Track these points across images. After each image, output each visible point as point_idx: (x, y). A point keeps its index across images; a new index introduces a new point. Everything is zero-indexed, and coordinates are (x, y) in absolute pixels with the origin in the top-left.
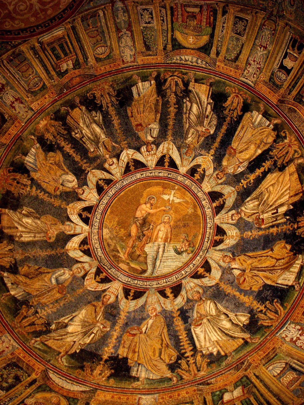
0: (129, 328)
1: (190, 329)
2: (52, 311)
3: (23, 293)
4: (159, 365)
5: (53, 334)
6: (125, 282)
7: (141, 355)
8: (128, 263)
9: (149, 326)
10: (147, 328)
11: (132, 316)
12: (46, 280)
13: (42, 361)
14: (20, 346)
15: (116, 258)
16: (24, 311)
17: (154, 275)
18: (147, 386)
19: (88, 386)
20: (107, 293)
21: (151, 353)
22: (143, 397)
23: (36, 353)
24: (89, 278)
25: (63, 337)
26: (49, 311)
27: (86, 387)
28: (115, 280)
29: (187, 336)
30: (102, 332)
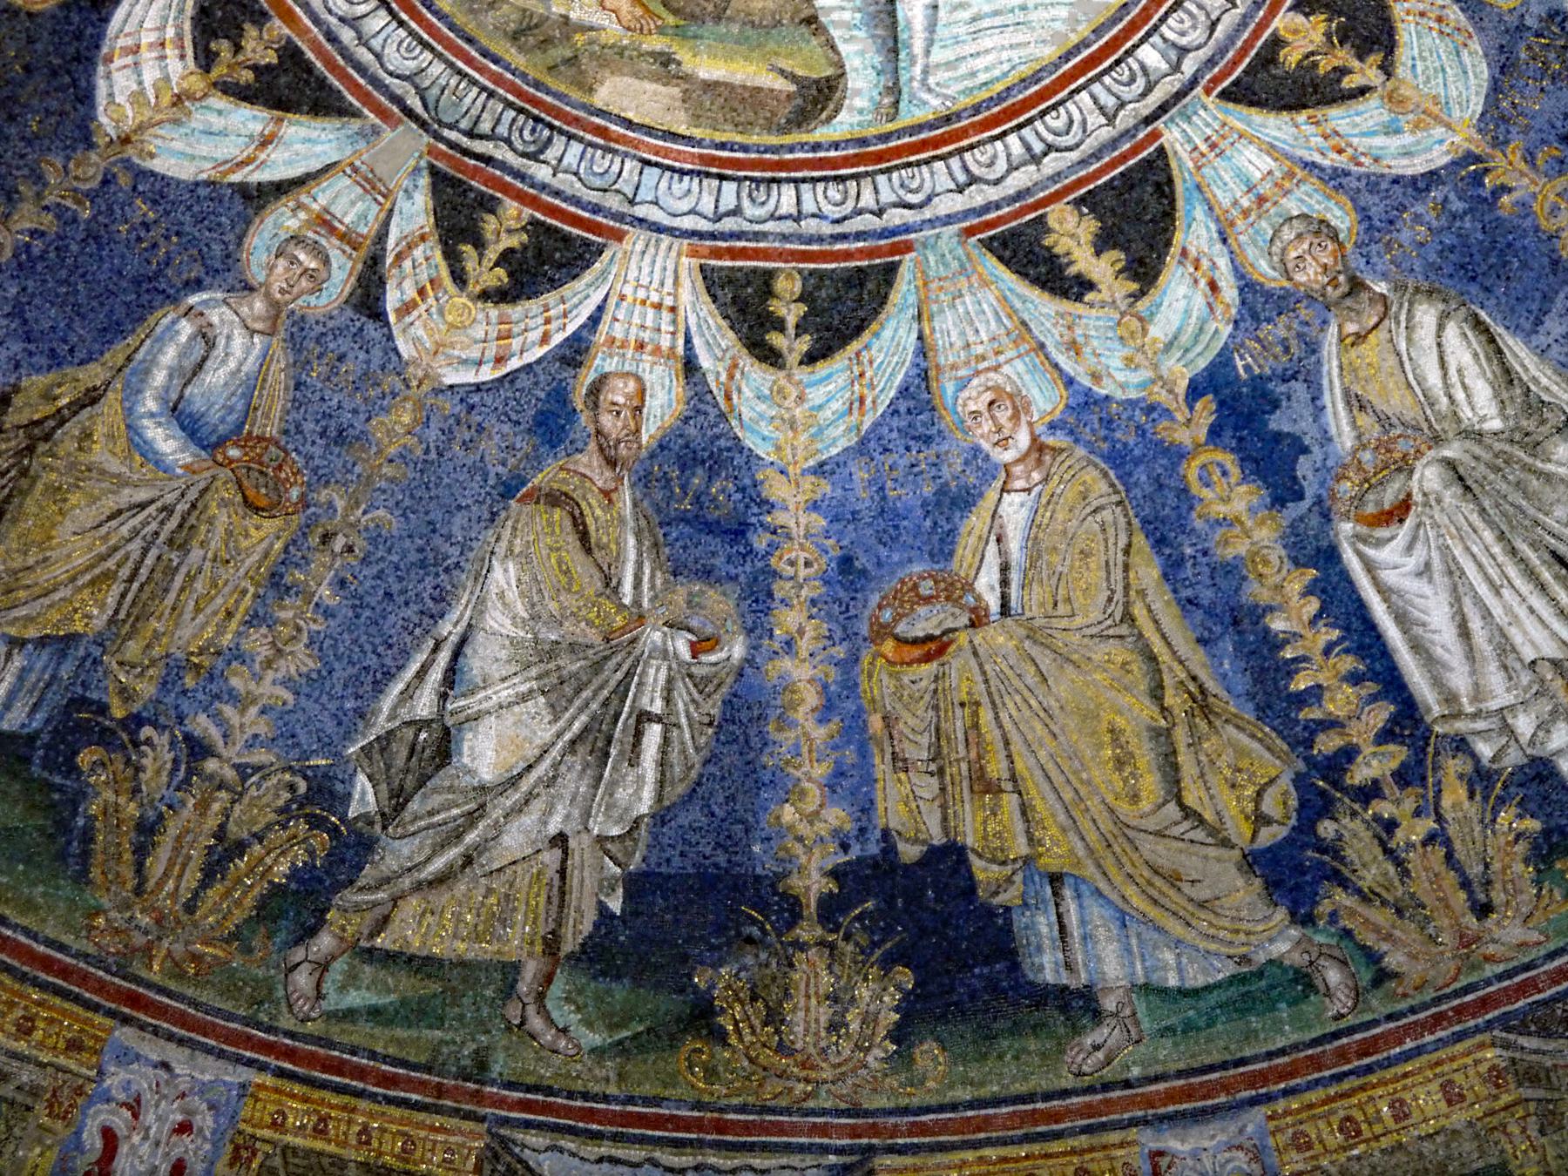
0: (875, 599)
1: (1330, 555)
2: (287, 682)
3: (18, 662)
4: (1190, 864)
5: (397, 852)
6: (704, 226)
7: (1043, 804)
8: (665, 60)
9: (1014, 546)
10: (1005, 569)
11: (863, 498)
12: (114, 466)
13: (440, 1091)
14: (250, 1063)
15: (546, 43)
16: (109, 795)
17: (911, 114)
18: (1168, 1055)
19: (802, 1149)
20: (601, 362)
21: (1102, 775)
22: (1173, 1143)
23: (373, 1055)
24: (410, 293)
25: (471, 837)
26: (270, 689)
27: (795, 1160)
28: (619, 236)
29: (1318, 616)
30: (701, 684)
